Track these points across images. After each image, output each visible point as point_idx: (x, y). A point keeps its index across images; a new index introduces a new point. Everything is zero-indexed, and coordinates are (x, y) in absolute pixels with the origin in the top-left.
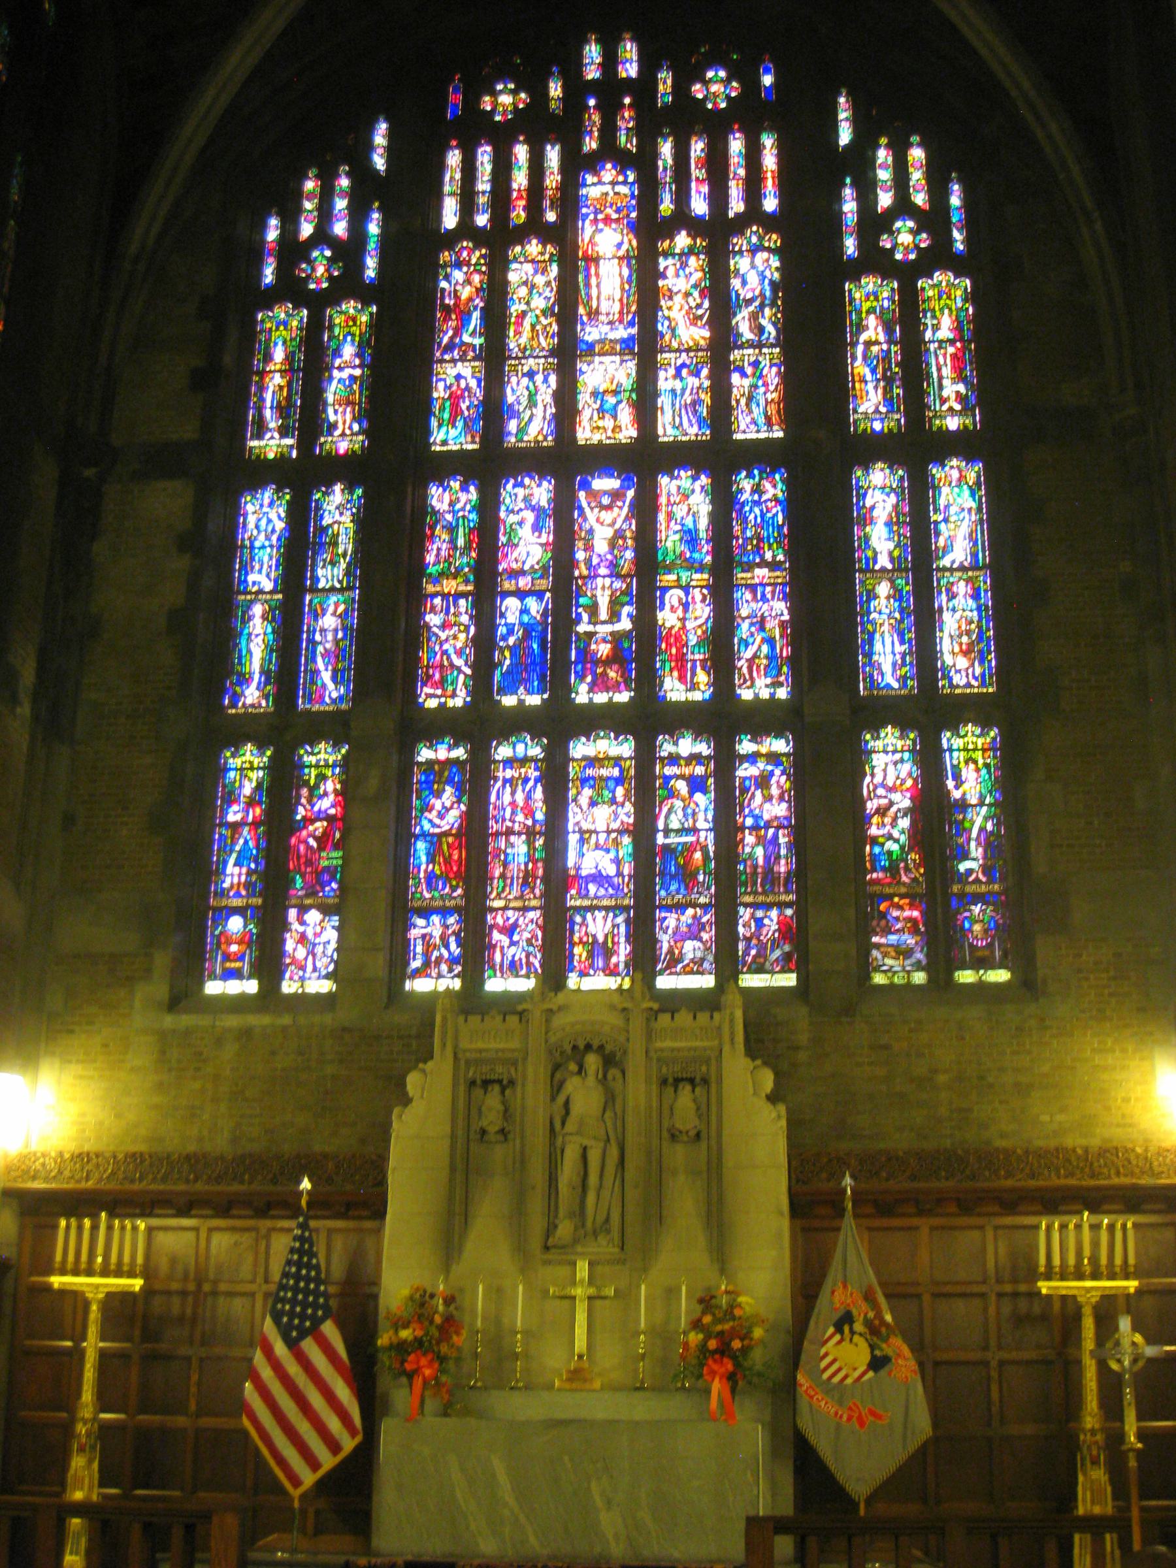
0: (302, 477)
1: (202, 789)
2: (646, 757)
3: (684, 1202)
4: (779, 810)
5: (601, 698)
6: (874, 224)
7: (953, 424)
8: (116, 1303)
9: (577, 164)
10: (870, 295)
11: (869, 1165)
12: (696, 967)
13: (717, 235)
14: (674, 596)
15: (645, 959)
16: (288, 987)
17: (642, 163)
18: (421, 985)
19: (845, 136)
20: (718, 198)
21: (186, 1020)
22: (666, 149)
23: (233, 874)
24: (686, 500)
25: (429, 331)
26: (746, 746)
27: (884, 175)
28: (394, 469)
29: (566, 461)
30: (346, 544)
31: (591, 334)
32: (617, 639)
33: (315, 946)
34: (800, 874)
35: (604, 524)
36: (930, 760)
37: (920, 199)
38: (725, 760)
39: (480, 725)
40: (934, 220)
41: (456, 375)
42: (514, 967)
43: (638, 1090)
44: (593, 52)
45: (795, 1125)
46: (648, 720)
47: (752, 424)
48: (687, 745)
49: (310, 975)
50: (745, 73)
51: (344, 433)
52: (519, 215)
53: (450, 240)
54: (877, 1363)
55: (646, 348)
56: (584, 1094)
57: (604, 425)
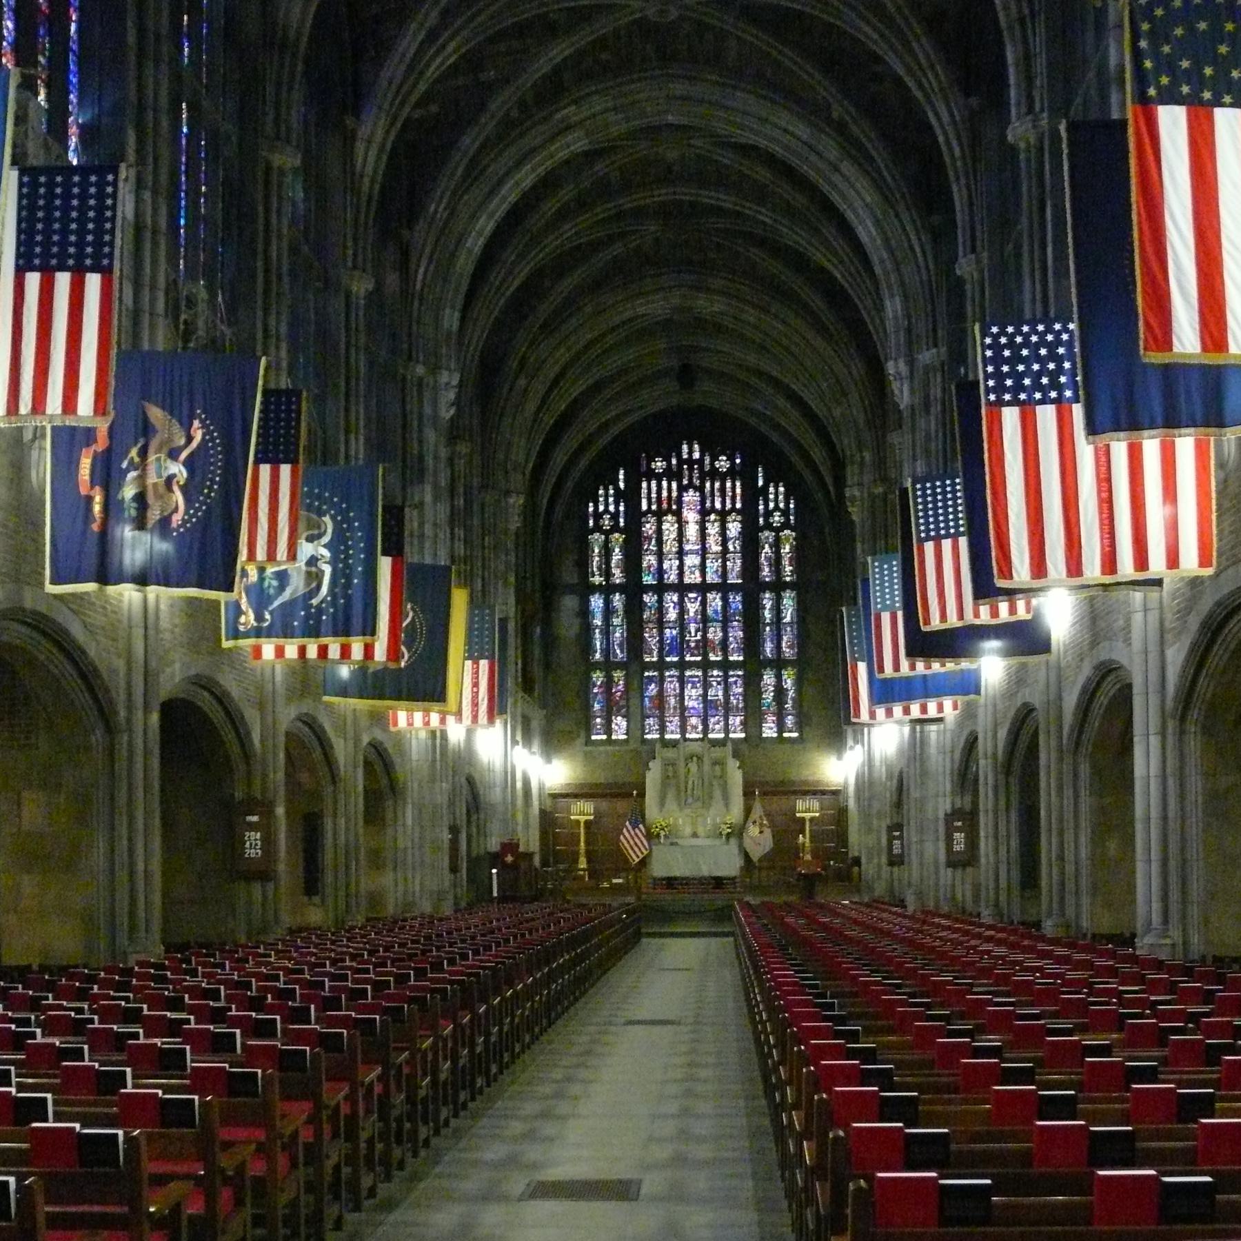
0: (607, 590)
1: (587, 683)
2: (705, 675)
3: (717, 793)
4: (740, 690)
5: (693, 659)
6: (768, 514)
7: (788, 579)
8: (586, 822)
9: (682, 489)
10: (767, 536)
11: (762, 784)
12: (719, 732)
13: (723, 515)
14: (712, 630)
15: (706, 731)
16: (614, 737)
17: (701, 489)
18: (648, 737)
19: (761, 483)
20: (723, 503)
21: (590, 748)
22: (708, 485)
23: (597, 707)
24: (715, 601)
25: (641, 545)
26: (731, 673)
27: (771, 497)
28: (633, 590)
29: (682, 588)
30: (621, 612)
31: (687, 547)
32: (697, 641)
33: (620, 725)
34: (745, 707)
35: (693, 608)
36: (779, 677)
37: (782, 505)
38: (726, 677)
39: (661, 666)
40: (785, 513)
41: (650, 560)
42: (672, 732)
43: (707, 767)
44: (685, 448)
45: (744, 773)
46: (706, 665)
47: (733, 579)
48: (715, 673)
49: (619, 734)
50: (731, 459)
51: (618, 576)
52: (665, 506)
53: (645, 514)
54: (761, 832)
55: (704, 552)
56: (693, 767)
57: (693, 578)
